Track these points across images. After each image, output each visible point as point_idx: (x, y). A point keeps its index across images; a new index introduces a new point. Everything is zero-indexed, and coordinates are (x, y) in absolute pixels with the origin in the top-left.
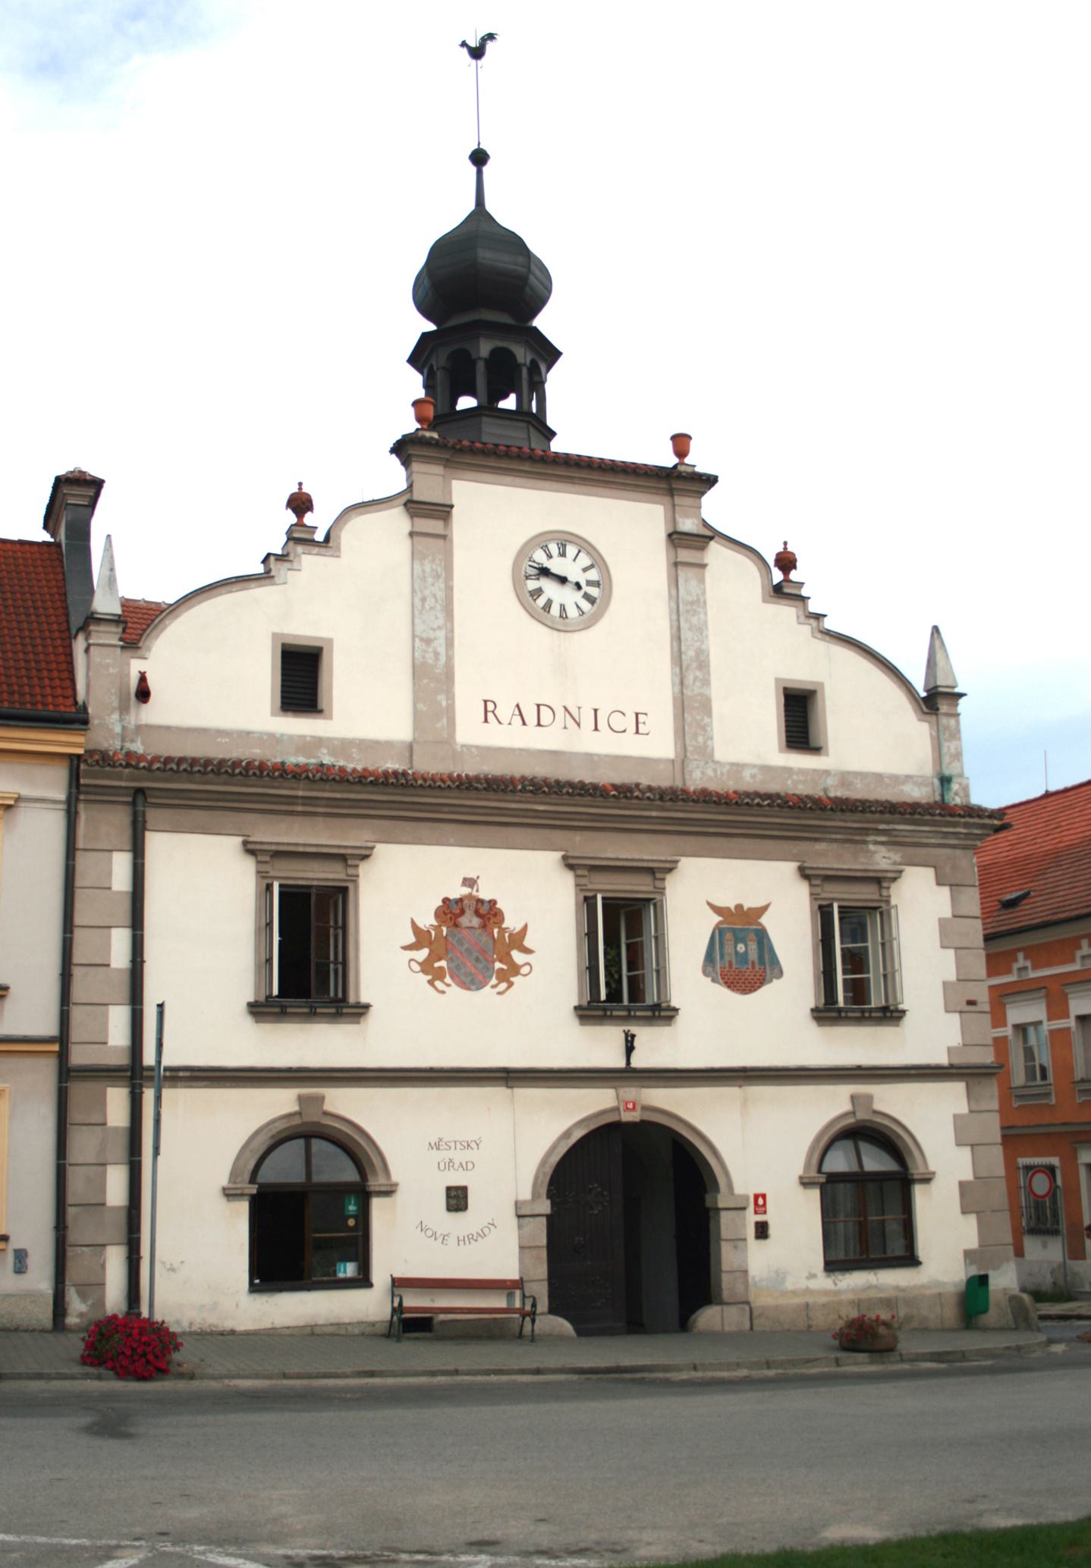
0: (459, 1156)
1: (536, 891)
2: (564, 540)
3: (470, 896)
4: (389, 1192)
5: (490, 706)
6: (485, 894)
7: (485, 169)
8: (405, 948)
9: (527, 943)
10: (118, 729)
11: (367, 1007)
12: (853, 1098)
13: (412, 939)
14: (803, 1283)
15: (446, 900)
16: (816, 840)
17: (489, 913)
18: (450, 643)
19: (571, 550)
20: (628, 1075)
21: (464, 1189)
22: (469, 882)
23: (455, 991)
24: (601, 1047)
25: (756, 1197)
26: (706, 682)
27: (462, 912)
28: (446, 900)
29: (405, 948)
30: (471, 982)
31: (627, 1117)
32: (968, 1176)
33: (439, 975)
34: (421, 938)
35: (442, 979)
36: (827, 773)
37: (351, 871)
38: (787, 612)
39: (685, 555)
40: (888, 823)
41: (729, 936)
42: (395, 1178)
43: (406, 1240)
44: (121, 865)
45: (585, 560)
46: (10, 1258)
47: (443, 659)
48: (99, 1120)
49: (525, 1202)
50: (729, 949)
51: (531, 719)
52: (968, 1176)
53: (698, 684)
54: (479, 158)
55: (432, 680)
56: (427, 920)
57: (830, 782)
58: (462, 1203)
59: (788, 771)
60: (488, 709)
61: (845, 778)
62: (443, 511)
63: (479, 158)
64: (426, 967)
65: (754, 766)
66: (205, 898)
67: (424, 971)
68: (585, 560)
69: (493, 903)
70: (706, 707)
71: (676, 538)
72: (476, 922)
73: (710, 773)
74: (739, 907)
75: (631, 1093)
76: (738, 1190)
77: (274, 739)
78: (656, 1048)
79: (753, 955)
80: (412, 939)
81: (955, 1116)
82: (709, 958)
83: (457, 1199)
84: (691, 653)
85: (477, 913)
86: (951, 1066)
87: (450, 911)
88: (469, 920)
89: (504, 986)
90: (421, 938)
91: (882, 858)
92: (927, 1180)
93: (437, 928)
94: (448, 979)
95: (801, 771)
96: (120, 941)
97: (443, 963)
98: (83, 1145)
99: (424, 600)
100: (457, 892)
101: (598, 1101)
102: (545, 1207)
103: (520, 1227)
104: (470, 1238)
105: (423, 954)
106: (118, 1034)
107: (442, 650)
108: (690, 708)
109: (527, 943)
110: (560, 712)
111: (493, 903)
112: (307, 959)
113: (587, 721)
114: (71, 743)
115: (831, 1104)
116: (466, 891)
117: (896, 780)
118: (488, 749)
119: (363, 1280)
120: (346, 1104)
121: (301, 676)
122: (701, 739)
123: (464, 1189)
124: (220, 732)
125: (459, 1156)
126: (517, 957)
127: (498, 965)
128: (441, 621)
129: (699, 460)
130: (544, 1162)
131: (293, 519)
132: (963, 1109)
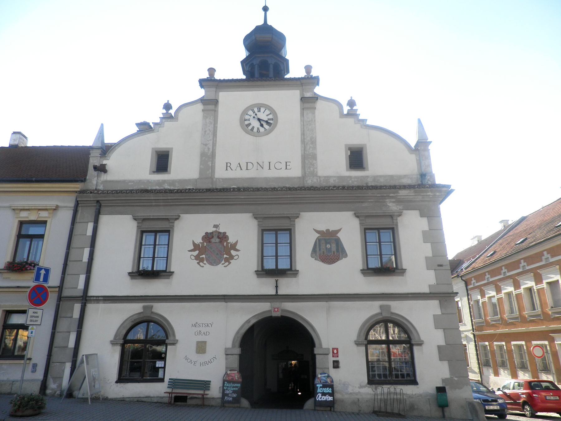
0: (203, 330)
1: (241, 229)
2: (259, 107)
3: (216, 231)
4: (173, 344)
5: (229, 165)
6: (221, 230)
7: (268, 13)
8: (189, 251)
9: (237, 247)
10: (95, 182)
11: (173, 272)
12: (381, 307)
13: (192, 248)
14: (357, 390)
15: (207, 233)
16: (362, 202)
17: (223, 237)
18: (214, 145)
19: (262, 110)
20: (277, 297)
21: (205, 342)
22: (216, 226)
23: (207, 266)
24: (266, 287)
25: (333, 349)
26: (315, 148)
27: (213, 237)
28: (207, 233)
29: (189, 251)
30: (214, 262)
31: (274, 314)
32: (442, 343)
33: (202, 260)
34: (196, 247)
35: (202, 261)
36: (368, 177)
37: (171, 224)
38: (351, 120)
39: (307, 105)
40: (394, 193)
41: (323, 242)
42: (177, 338)
43: (180, 364)
44: (90, 226)
45: (268, 112)
46: (31, 366)
47: (211, 150)
48: (69, 315)
49: (228, 349)
50: (323, 247)
51: (244, 167)
52: (442, 343)
53: (311, 149)
54: (265, 9)
55: (208, 158)
56: (199, 240)
57: (369, 180)
59: (350, 177)
60: (228, 166)
61: (375, 178)
62: (215, 102)
63: (265, 9)
64: (197, 257)
65: (335, 177)
66: (118, 235)
67: (196, 259)
68: (268, 112)
69: (225, 233)
70: (314, 157)
71: (303, 99)
72: (218, 240)
73: (315, 180)
74: (328, 230)
75: (277, 304)
76: (324, 346)
77: (149, 182)
78: (288, 286)
79: (334, 248)
80: (192, 248)
81: (434, 315)
82: (314, 250)
83: (201, 348)
84: (309, 139)
85: (218, 237)
86: (430, 293)
87: (208, 237)
88: (215, 240)
89: (227, 263)
90: (196, 247)
91: (393, 207)
92: (420, 344)
93: (202, 244)
94: (205, 262)
95: (356, 177)
96: (86, 252)
97: (204, 256)
98: (63, 325)
99: (205, 132)
100: (211, 230)
101: (263, 307)
102: (238, 351)
103: (226, 359)
104: (206, 363)
105: (197, 252)
106: (81, 286)
107: (211, 147)
108: (308, 158)
109: (237, 247)
110: (255, 164)
111: (225, 233)
113: (266, 166)
114: (77, 186)
115: (372, 309)
116: (215, 229)
117: (400, 177)
118: (226, 179)
119: (162, 380)
120: (160, 309)
121: (162, 161)
122: (312, 169)
123: (205, 342)
124: (130, 181)
125: (203, 330)
126: (233, 253)
127: (225, 256)
128: (211, 138)
129: (314, 73)
130: (238, 332)
131: (164, 111)
132: (438, 312)
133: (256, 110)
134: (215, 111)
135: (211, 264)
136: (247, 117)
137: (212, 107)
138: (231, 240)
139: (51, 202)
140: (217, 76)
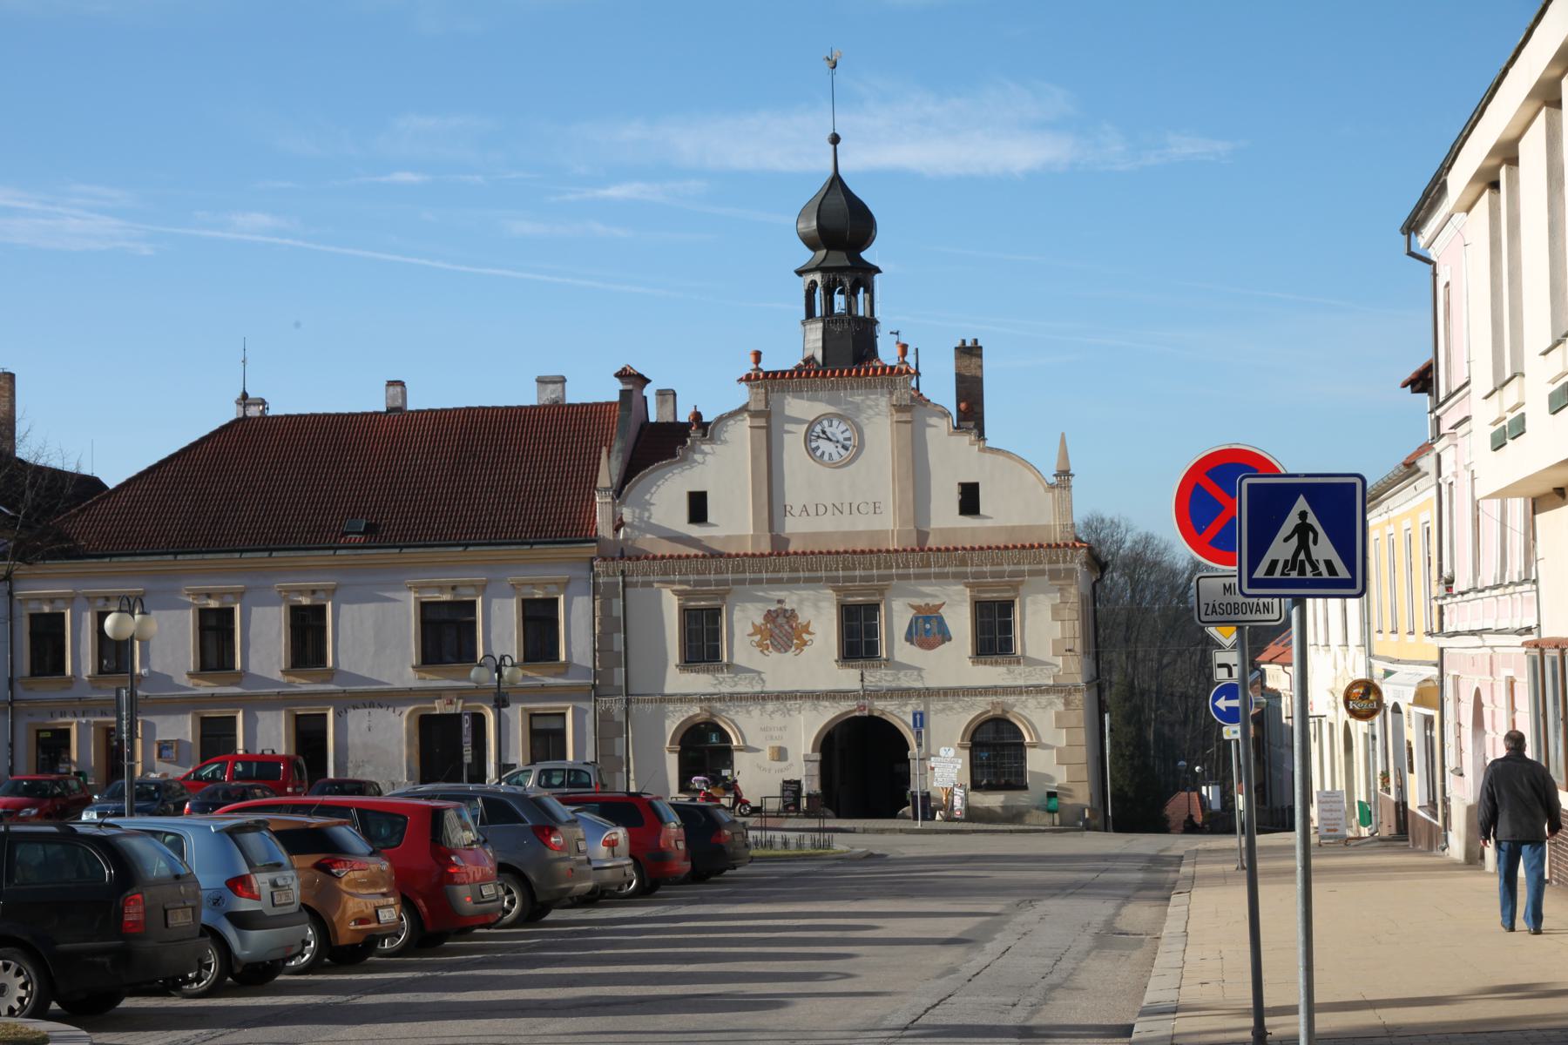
0: (776, 733)
17: (791, 616)
19: (835, 423)
24: (849, 678)
54: (835, 139)
58: (775, 753)
63: (835, 139)
64: (759, 645)
78: (879, 678)
88: (781, 620)
102: (817, 756)
112: (702, 643)
115: (980, 707)
121: (698, 507)
125: (776, 733)
126: (806, 637)
133: (825, 423)
134: (768, 428)
135: (779, 650)
136: (814, 445)
137: (762, 422)
138: (802, 619)
139: (561, 574)
140: (766, 366)
